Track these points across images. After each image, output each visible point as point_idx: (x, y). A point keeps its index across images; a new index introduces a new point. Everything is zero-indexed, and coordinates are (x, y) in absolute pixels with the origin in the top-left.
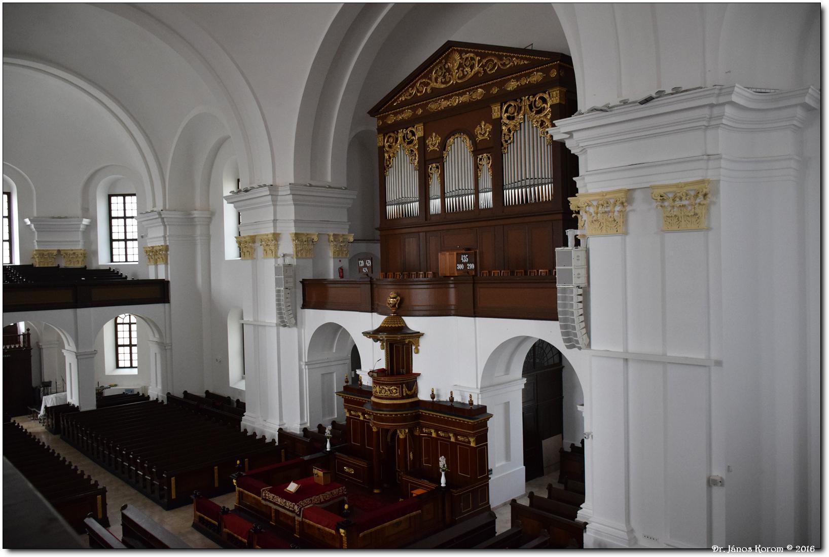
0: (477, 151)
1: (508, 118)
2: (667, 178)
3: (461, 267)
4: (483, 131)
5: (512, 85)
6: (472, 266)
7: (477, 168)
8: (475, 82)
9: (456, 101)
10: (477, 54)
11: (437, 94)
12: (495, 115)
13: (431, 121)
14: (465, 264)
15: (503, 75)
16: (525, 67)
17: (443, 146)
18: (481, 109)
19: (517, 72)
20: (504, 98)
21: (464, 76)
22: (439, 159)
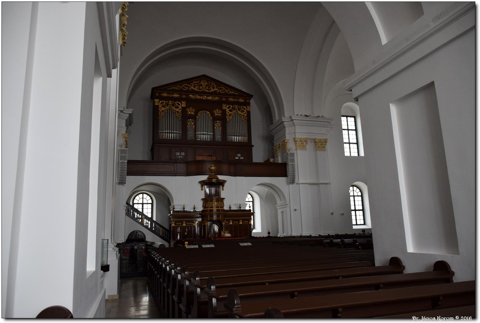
0: (215, 119)
1: (229, 111)
2: (318, 137)
3: (237, 158)
4: (217, 113)
5: (231, 100)
6: (242, 158)
7: (214, 126)
8: (214, 94)
9: (205, 97)
10: (216, 84)
11: (194, 92)
12: (224, 108)
13: (190, 102)
14: (239, 157)
15: (228, 95)
16: (237, 95)
17: (196, 113)
18: (218, 104)
19: (233, 96)
20: (228, 103)
21: (209, 90)
22: (194, 117)
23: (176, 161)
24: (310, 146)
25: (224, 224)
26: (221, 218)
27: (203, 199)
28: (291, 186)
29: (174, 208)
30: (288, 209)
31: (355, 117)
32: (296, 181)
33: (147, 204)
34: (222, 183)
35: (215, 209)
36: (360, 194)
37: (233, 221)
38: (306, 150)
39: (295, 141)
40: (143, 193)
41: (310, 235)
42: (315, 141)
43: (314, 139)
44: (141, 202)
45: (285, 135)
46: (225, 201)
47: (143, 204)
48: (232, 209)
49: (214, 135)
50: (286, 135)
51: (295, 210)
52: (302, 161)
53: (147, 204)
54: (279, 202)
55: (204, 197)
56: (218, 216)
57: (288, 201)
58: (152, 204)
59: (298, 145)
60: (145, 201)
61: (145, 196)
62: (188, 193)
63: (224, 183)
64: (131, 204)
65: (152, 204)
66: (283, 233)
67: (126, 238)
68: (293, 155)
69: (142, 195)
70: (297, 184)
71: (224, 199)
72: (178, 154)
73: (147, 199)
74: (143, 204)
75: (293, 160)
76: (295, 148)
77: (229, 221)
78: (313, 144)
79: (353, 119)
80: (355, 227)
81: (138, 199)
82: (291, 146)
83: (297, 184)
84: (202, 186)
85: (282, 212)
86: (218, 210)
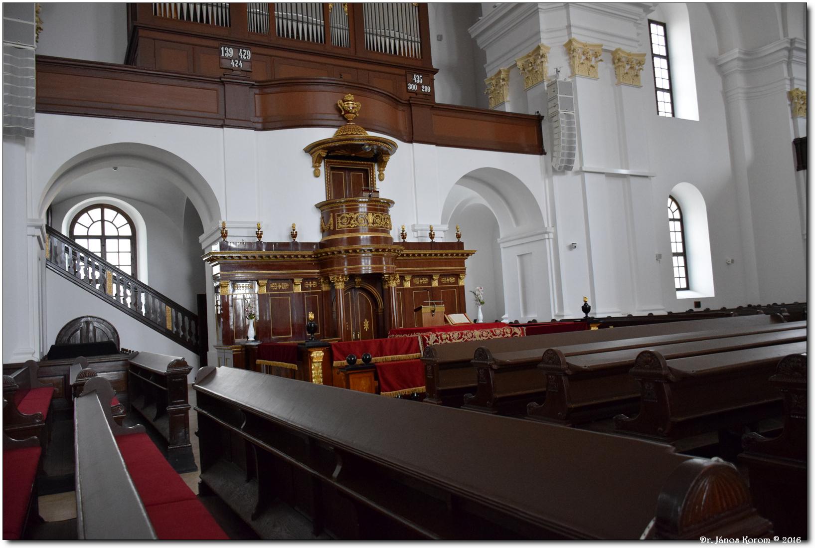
3: (412, 87)
14: (419, 85)
23: (225, 79)
24: (605, 69)
25: (393, 284)
26: (385, 267)
27: (320, 206)
28: (556, 179)
29: (224, 235)
30: (549, 244)
31: (664, 25)
32: (576, 166)
33: (118, 237)
34: (380, 156)
35: (364, 236)
36: (677, 215)
37: (414, 276)
38: (597, 79)
39: (569, 48)
40: (102, 206)
41: (517, 321)
42: (616, 59)
43: (614, 53)
44: (96, 230)
45: (538, 33)
46: (392, 211)
47: (103, 238)
48: (409, 239)
49: (327, 26)
50: (543, 35)
51: (573, 247)
52: (589, 108)
53: (118, 237)
54: (506, 229)
55: (323, 198)
56: (376, 260)
57: (547, 223)
58: (133, 239)
59: (577, 62)
60: (110, 231)
61: (109, 214)
62: (264, 184)
63: (388, 154)
64: (65, 231)
65: (133, 239)
66: (526, 311)
67: (51, 341)
68: (569, 88)
69: (99, 210)
70: (577, 173)
71: (389, 203)
72: (230, 52)
73: (117, 224)
74: (103, 238)
75: (570, 104)
76: (569, 73)
77: (402, 278)
78: (611, 65)
79: (661, 28)
80: (681, 295)
81: (88, 224)
82: (555, 64)
83: (581, 172)
84: (317, 162)
85: (521, 256)
86: (374, 240)
